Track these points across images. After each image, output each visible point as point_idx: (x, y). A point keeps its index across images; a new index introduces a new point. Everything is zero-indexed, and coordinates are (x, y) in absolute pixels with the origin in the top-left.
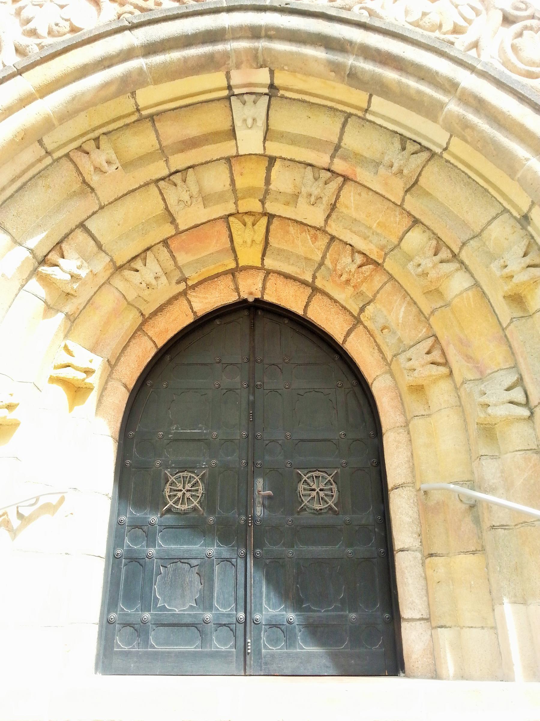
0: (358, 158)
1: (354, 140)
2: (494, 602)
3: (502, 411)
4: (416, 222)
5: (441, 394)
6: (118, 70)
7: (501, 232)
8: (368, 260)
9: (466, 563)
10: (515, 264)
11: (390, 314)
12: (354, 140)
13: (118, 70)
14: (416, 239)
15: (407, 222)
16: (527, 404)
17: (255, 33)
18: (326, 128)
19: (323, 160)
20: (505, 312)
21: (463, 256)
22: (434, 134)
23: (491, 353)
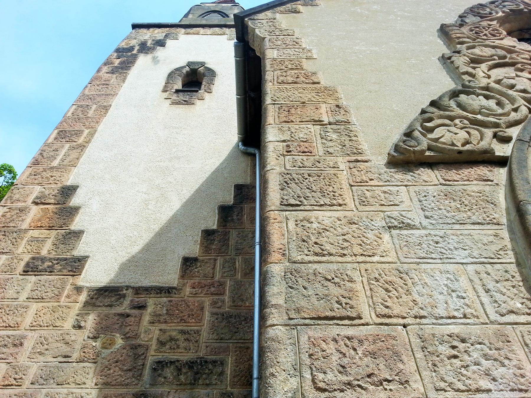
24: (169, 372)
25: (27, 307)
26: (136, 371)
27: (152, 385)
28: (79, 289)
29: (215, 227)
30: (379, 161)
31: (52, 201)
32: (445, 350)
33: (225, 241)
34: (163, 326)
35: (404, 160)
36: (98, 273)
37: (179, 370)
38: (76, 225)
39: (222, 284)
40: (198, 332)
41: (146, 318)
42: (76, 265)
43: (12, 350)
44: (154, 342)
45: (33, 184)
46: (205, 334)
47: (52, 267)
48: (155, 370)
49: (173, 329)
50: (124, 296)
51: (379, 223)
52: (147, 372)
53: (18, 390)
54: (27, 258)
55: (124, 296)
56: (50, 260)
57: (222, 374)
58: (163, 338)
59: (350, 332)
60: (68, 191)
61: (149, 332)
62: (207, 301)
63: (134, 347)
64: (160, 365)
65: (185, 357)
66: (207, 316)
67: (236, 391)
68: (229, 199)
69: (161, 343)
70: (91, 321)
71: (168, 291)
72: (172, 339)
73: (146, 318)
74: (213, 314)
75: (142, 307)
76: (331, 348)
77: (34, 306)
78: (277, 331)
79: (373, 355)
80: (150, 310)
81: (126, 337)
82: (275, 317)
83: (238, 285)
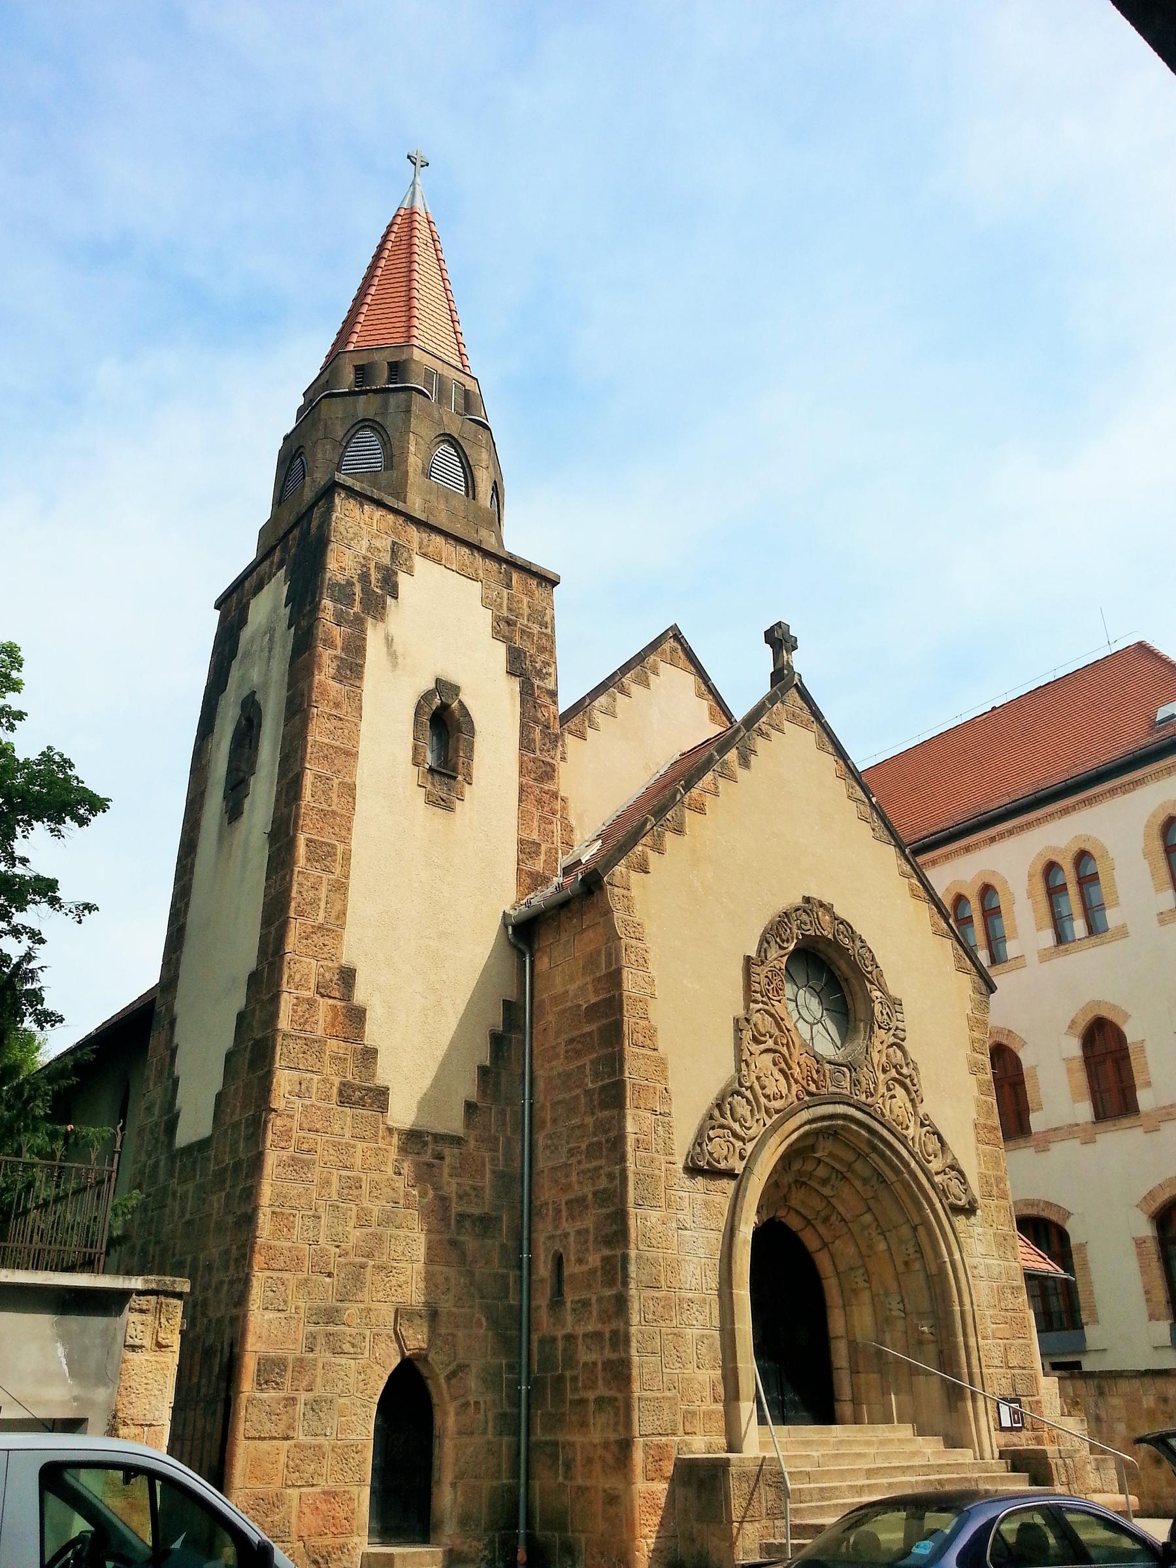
0: (853, 1171)
1: (858, 1166)
2: (885, 1393)
3: (896, 1313)
4: (869, 1209)
5: (866, 1297)
6: (802, 1130)
7: (905, 1230)
8: (843, 1220)
9: (874, 1377)
10: (911, 1251)
11: (846, 1250)
12: (858, 1166)
13: (802, 1130)
14: (868, 1218)
15: (865, 1209)
16: (904, 1311)
17: (845, 1117)
18: (850, 1156)
19: (844, 1170)
20: (901, 1268)
21: (888, 1234)
22: (890, 1175)
23: (893, 1285)
24: (467, 1224)
25: (354, 1147)
26: (445, 1219)
27: (458, 1234)
28: (390, 1130)
29: (488, 1063)
30: (680, 1161)
31: (337, 995)
32: (685, 1305)
33: (497, 1084)
34: (459, 1180)
35: (693, 1170)
36: (403, 1112)
37: (474, 1224)
38: (368, 1041)
39: (497, 1139)
40: (483, 1188)
41: (446, 1171)
42: (379, 1097)
43: (355, 1192)
44: (454, 1196)
45: (307, 955)
46: (488, 1193)
47: (362, 1098)
48: (458, 1222)
49: (467, 1181)
50: (425, 1144)
51: (674, 1225)
52: (453, 1222)
53: (370, 1230)
54: (336, 1080)
55: (425, 1144)
56: (360, 1088)
57: (500, 1229)
58: (461, 1192)
59: (657, 1295)
60: (347, 976)
61: (451, 1186)
62: (487, 1156)
63: (443, 1199)
64: (462, 1217)
65: (476, 1211)
66: (488, 1175)
67: (509, 1244)
68: (496, 1019)
69: (460, 1197)
70: (407, 1167)
71: (456, 1141)
72: (466, 1194)
73: (446, 1171)
74: (493, 1172)
75: (442, 1158)
76: (651, 1303)
77: (360, 1145)
78: (633, 1292)
79: (663, 1307)
80: (447, 1160)
81: (435, 1189)
82: (632, 1285)
83: (508, 1141)
